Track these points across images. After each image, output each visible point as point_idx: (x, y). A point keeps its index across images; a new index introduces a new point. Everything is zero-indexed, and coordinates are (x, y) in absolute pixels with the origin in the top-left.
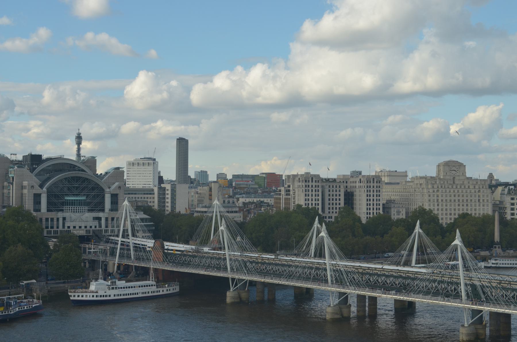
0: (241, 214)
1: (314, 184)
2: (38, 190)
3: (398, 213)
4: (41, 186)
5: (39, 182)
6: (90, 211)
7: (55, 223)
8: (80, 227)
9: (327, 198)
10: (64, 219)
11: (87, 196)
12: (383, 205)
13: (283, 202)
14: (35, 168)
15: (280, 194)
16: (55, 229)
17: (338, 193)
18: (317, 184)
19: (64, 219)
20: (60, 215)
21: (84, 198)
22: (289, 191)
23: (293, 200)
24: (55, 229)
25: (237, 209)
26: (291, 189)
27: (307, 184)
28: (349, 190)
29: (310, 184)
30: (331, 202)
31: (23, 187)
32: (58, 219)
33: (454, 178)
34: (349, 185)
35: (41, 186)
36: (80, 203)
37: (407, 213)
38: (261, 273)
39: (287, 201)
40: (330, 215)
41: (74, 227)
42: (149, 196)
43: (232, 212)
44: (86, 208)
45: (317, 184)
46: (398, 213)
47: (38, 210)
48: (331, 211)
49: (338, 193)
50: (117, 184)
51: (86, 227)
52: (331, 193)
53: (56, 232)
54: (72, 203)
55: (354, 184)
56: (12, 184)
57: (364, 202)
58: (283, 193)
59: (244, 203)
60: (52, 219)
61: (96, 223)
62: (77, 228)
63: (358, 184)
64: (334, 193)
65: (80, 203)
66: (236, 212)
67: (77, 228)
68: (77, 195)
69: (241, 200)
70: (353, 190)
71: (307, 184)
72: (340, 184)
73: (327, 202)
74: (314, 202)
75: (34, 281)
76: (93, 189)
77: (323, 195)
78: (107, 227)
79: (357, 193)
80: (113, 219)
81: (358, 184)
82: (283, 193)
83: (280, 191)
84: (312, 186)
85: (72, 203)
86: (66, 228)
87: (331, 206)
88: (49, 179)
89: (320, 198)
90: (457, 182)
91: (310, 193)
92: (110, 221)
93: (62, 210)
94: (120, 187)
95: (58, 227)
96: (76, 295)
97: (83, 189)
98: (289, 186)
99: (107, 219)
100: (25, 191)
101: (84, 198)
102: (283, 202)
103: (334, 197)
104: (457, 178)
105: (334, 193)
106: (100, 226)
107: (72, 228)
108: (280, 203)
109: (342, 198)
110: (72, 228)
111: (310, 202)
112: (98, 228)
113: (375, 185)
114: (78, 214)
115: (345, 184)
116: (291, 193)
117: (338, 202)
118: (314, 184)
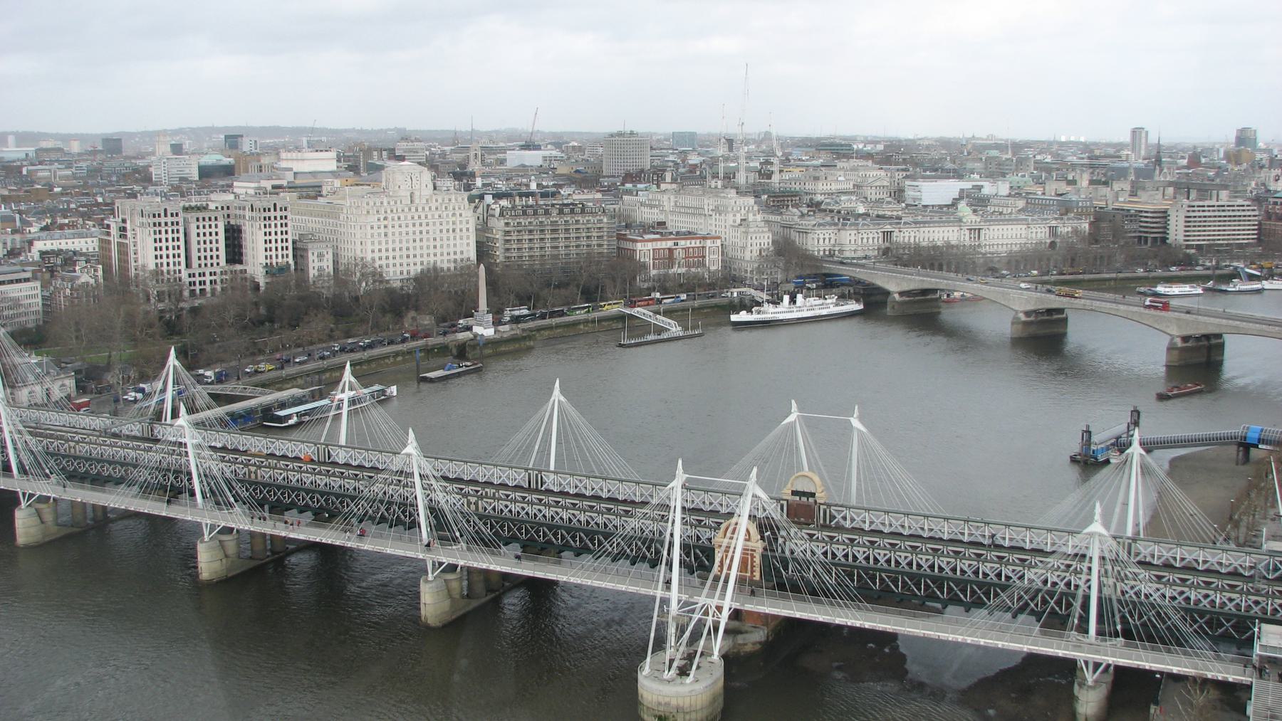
0: (38, 284)
1: (169, 219)
3: (320, 256)
9: (194, 239)
12: (294, 242)
13: (114, 248)
15: (108, 234)
18: (175, 219)
22: (124, 229)
23: (132, 248)
25: (28, 275)
26: (128, 226)
27: (157, 220)
28: (233, 222)
29: (163, 220)
30: (202, 246)
33: (412, 195)
37: (336, 263)
38: (74, 477)
39: (123, 249)
40: (201, 271)
43: (18, 281)
45: (175, 219)
46: (320, 256)
49: (213, 230)
55: (241, 212)
57: (261, 246)
58: (114, 231)
59: (42, 253)
63: (248, 214)
66: (27, 280)
69: (39, 246)
71: (157, 220)
72: (216, 214)
73: (194, 247)
82: (114, 231)
83: (108, 227)
84: (166, 224)
87: (203, 254)
89: (182, 243)
90: (417, 201)
91: (163, 236)
98: (124, 221)
102: (114, 248)
104: (417, 194)
105: (207, 230)
108: (110, 250)
111: (165, 260)
113: (279, 214)
115: (226, 212)
116: (129, 234)
117: (214, 245)
118: (169, 219)
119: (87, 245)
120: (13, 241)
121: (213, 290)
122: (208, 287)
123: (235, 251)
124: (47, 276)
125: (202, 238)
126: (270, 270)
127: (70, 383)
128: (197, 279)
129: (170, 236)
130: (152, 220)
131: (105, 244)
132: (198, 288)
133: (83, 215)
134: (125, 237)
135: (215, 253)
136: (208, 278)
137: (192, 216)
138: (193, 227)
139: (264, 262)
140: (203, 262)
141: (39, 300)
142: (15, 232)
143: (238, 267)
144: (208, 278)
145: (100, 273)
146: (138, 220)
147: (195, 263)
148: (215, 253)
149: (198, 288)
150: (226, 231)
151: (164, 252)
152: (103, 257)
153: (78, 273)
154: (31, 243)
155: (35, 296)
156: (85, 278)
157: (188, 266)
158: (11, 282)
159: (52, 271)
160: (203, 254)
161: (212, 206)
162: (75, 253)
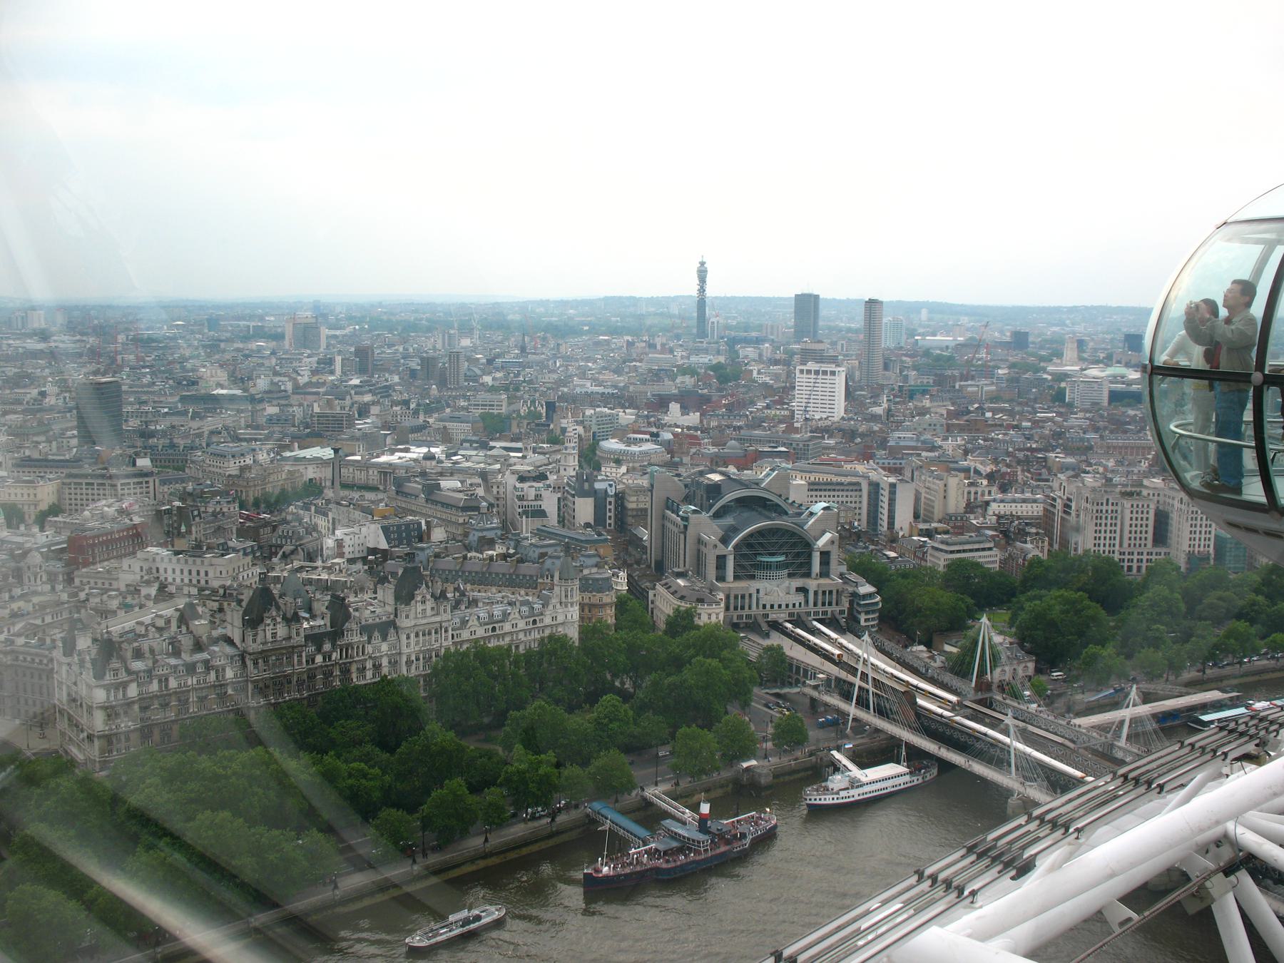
1: (1110, 508)
2: (721, 550)
4: (725, 541)
5: (721, 533)
6: (790, 575)
7: (747, 600)
8: (780, 606)
10: (758, 591)
11: (787, 555)
14: (711, 506)
15: (1054, 506)
16: (746, 612)
17: (1145, 516)
18: (1114, 508)
19: (758, 591)
20: (753, 586)
21: (782, 558)
22: (1070, 507)
24: (746, 612)
25: (992, 545)
26: (1073, 505)
27: (1100, 508)
29: (1104, 508)
31: (700, 541)
32: (750, 595)
34: (1161, 498)
35: (725, 541)
36: (779, 566)
41: (772, 606)
42: (853, 494)
43: (983, 549)
44: (786, 571)
45: (1114, 508)
47: (721, 578)
48: (1133, 542)
50: (828, 536)
51: (787, 606)
52: (1134, 515)
53: (748, 617)
54: (768, 566)
56: (685, 533)
57: (1186, 534)
59: (999, 517)
60: (743, 597)
61: (800, 598)
62: (776, 607)
63: (1176, 504)
64: (1140, 516)
65: (779, 566)
66: (990, 549)
67: (776, 607)
68: (772, 555)
69: (994, 507)
70: (1167, 508)
71: (1100, 508)
73: (1127, 528)
74: (1107, 549)
75: (753, 762)
76: (794, 545)
77: (1122, 531)
78: (815, 604)
79: (1174, 516)
80: (824, 593)
81: (1176, 504)
83: (1054, 500)
85: (768, 566)
86: (761, 611)
88: (734, 530)
92: (820, 597)
93: (752, 577)
94: (833, 542)
95: (750, 608)
96: (815, 797)
97: (781, 546)
99: (816, 593)
100: (702, 548)
101: (782, 558)
102: (1057, 519)
103: (1139, 522)
105: (1140, 516)
106: (807, 602)
107: (768, 607)
109: (1151, 523)
110: (768, 607)
112: (804, 609)
114: (774, 582)
116: (1073, 513)
118: (1110, 508)
119: (1036, 510)
120: (969, 493)
121: (1139, 568)
122: (1135, 565)
123: (1161, 533)
124: (1003, 542)
125: (1134, 522)
126: (1190, 556)
127: (1031, 665)
128: (1127, 557)
129: (1109, 522)
130: (1095, 508)
131: (1048, 514)
132: (1126, 564)
133: (1019, 462)
134: (1069, 514)
135: (1143, 535)
136: (1135, 557)
137: (1127, 504)
138: (1127, 512)
139: (1187, 549)
140: (1133, 542)
141: (997, 565)
142: (971, 484)
143: (1163, 550)
144: (1135, 557)
145: (1046, 543)
146: (1084, 504)
147: (1125, 544)
148: (1143, 535)
149: (1126, 564)
150: (1156, 515)
151: (1102, 535)
152: (1045, 523)
153: (1029, 546)
154: (987, 503)
155: (994, 562)
156: (1036, 552)
157: (1121, 545)
158: (977, 550)
159: (1005, 533)
160: (1133, 529)
161: (1145, 492)
162: (1027, 524)
